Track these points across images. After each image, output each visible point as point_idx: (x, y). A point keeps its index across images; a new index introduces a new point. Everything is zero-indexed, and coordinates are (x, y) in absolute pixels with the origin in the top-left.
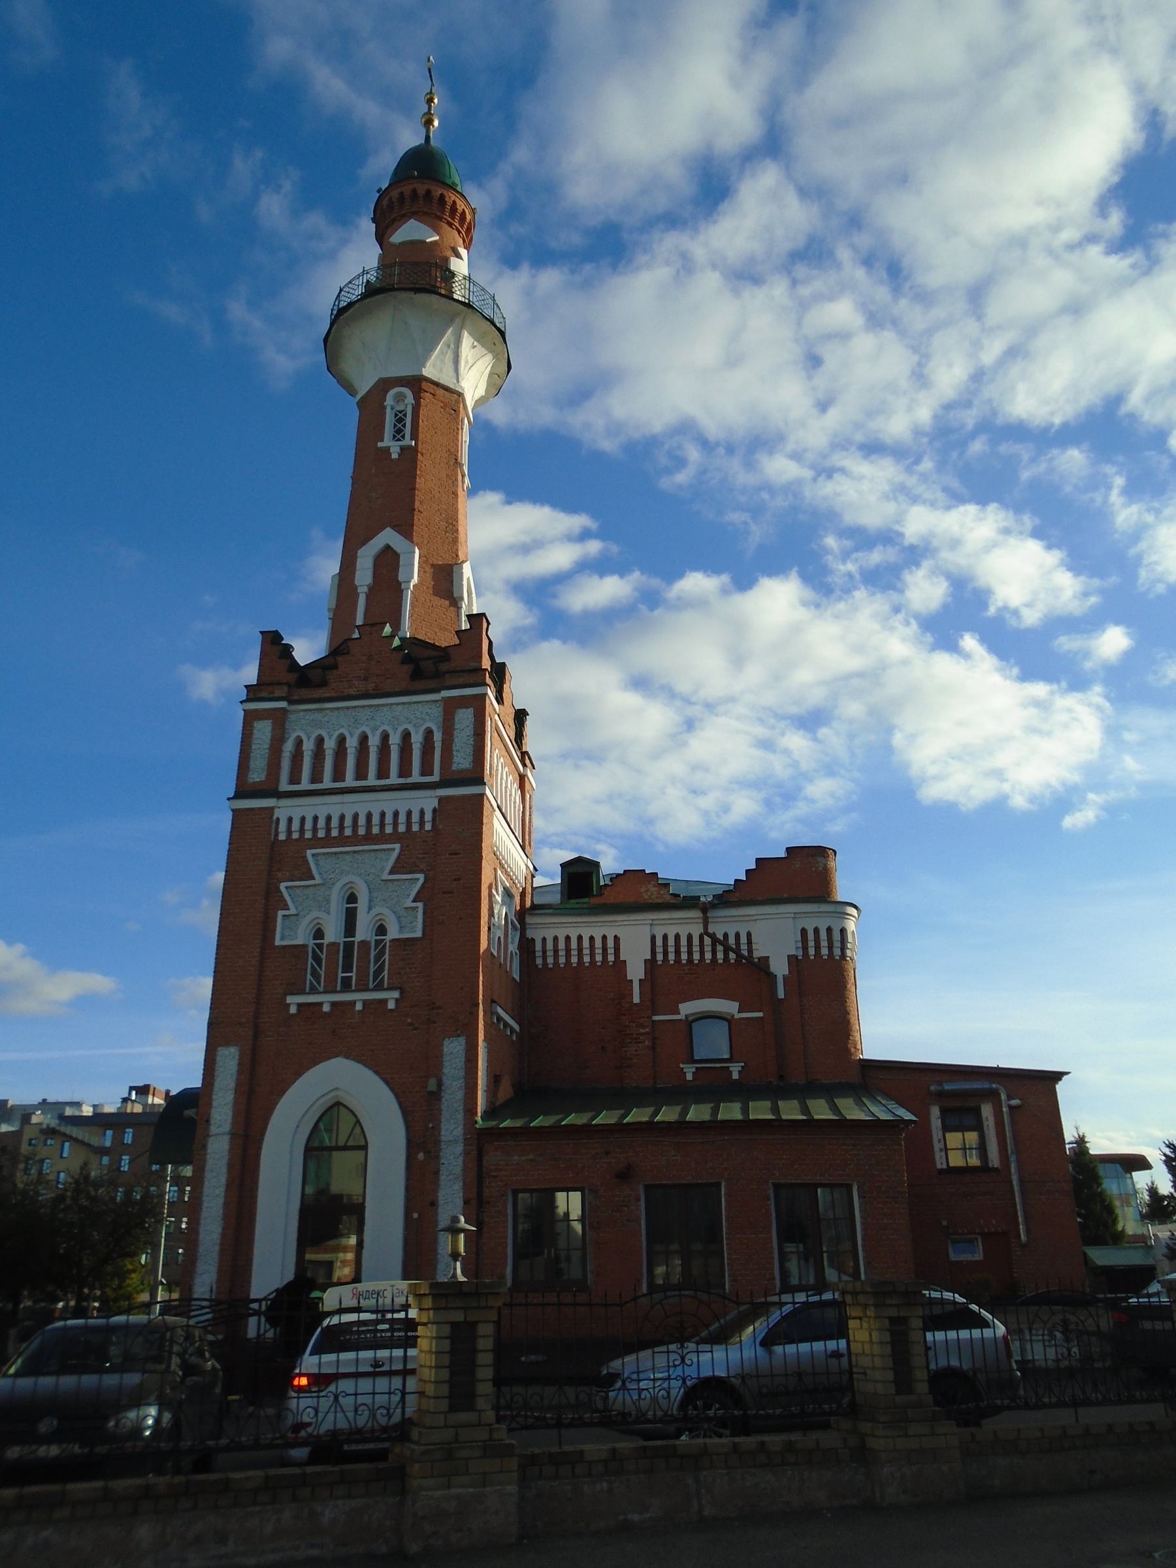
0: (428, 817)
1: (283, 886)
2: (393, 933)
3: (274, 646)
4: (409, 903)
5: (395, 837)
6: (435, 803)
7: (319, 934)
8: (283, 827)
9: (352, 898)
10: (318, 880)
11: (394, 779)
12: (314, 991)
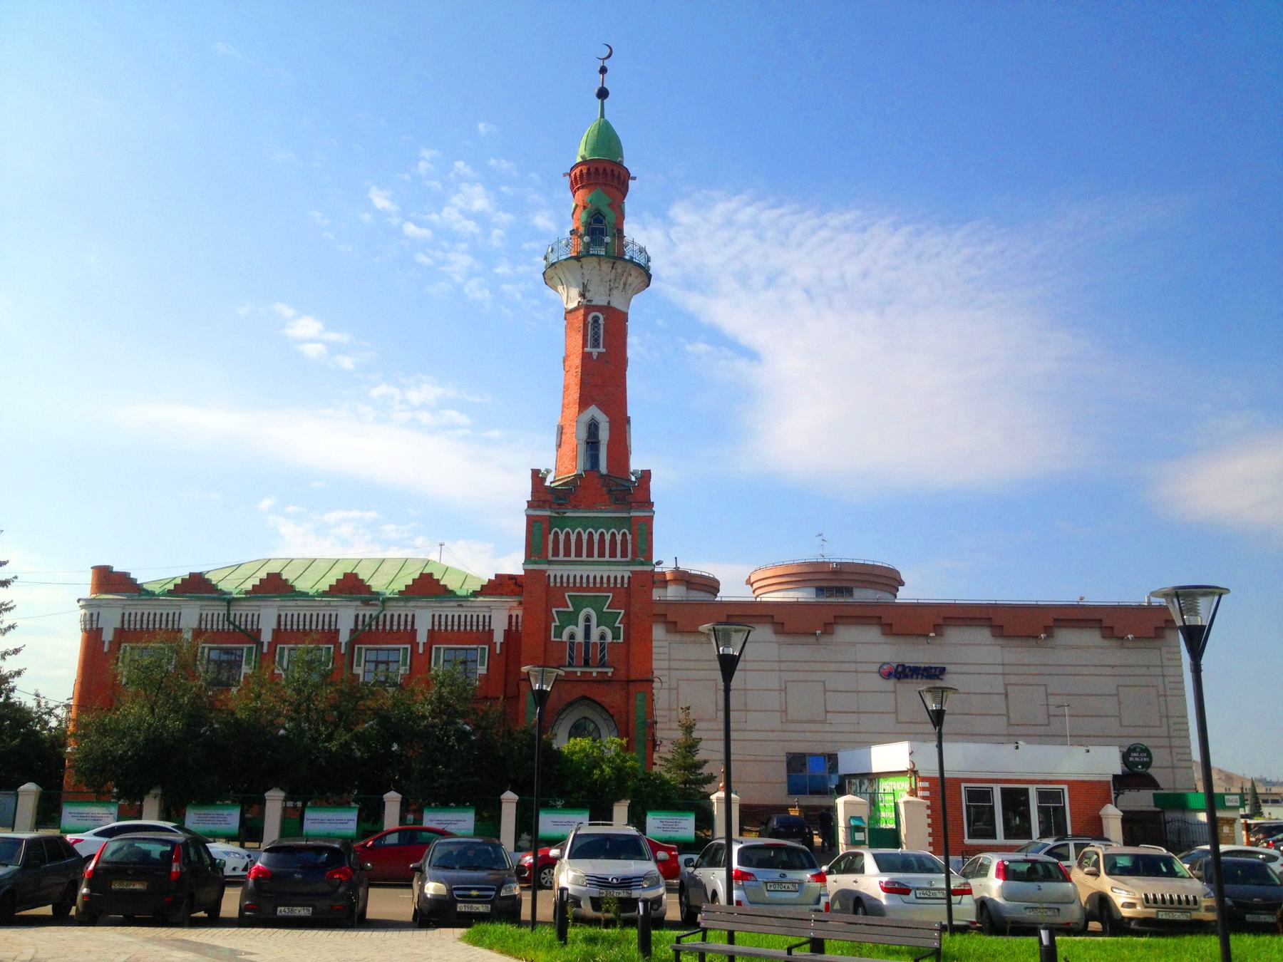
0: (626, 580)
1: (554, 610)
2: (609, 639)
3: (537, 477)
4: (617, 625)
5: (609, 589)
6: (626, 575)
7: (572, 636)
8: (552, 579)
9: (588, 619)
10: (571, 609)
11: (607, 558)
12: (570, 665)
